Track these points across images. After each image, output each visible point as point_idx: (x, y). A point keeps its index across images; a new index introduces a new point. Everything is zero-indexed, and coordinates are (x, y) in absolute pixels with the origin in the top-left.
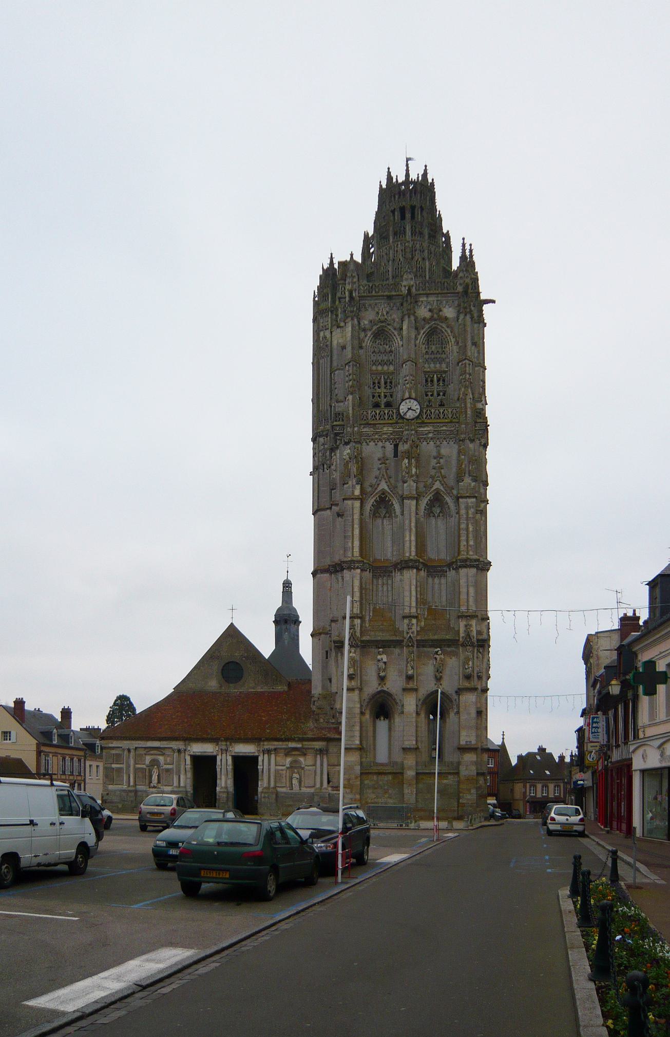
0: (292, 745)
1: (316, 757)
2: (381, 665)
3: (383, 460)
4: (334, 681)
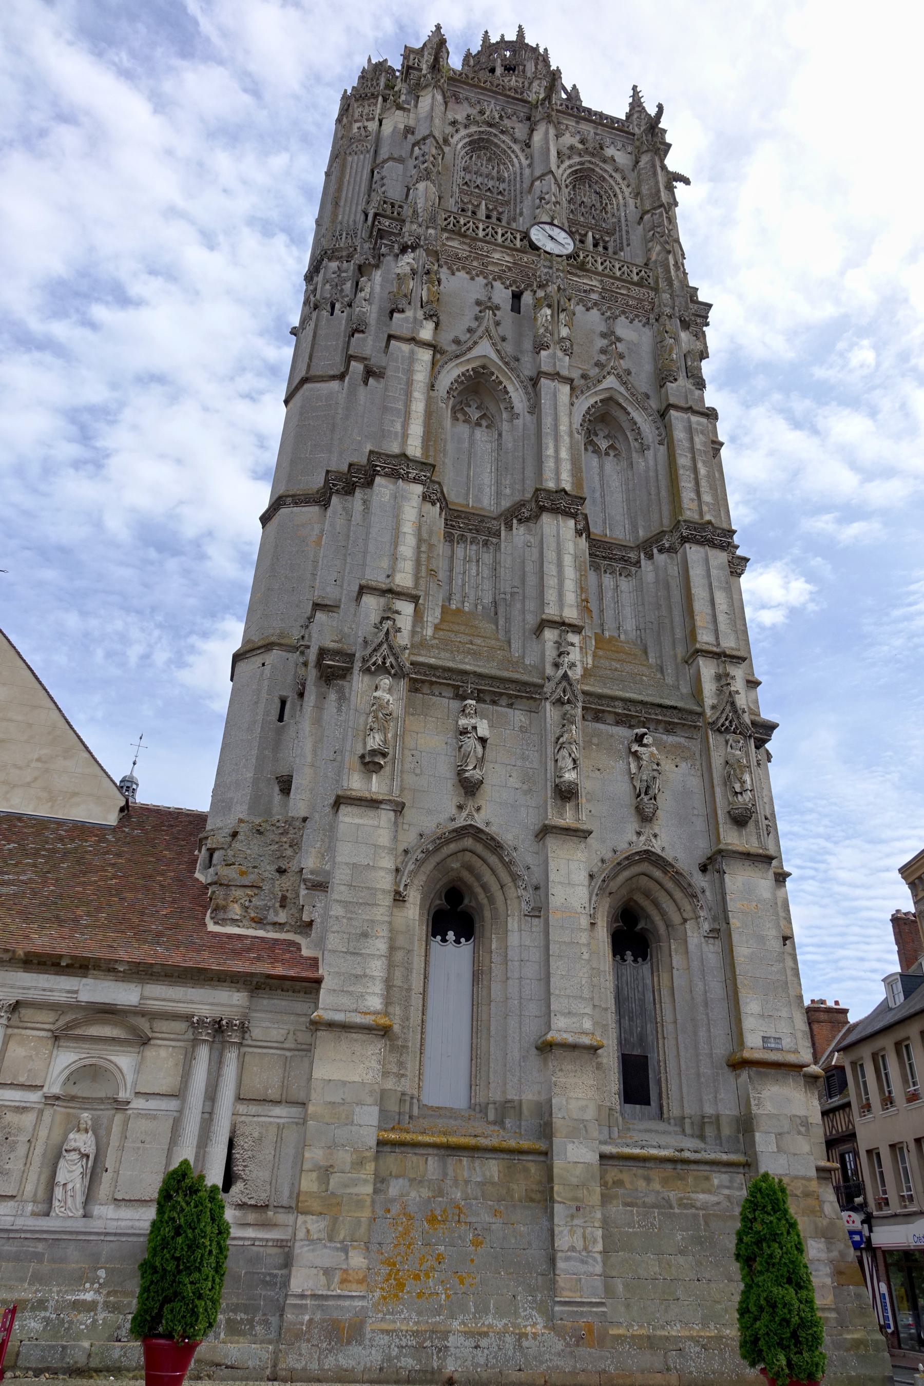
1: (189, 1059)
2: (471, 743)
3: (486, 305)
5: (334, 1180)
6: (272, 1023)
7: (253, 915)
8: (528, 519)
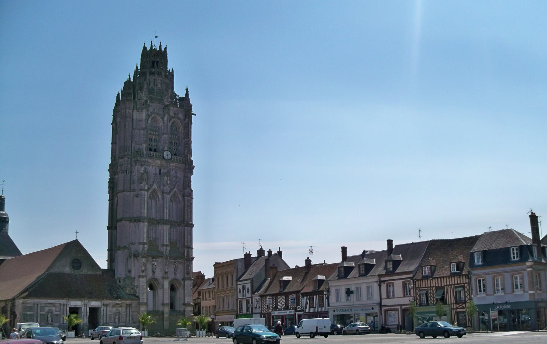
4: (133, 272)
6: (135, 303)
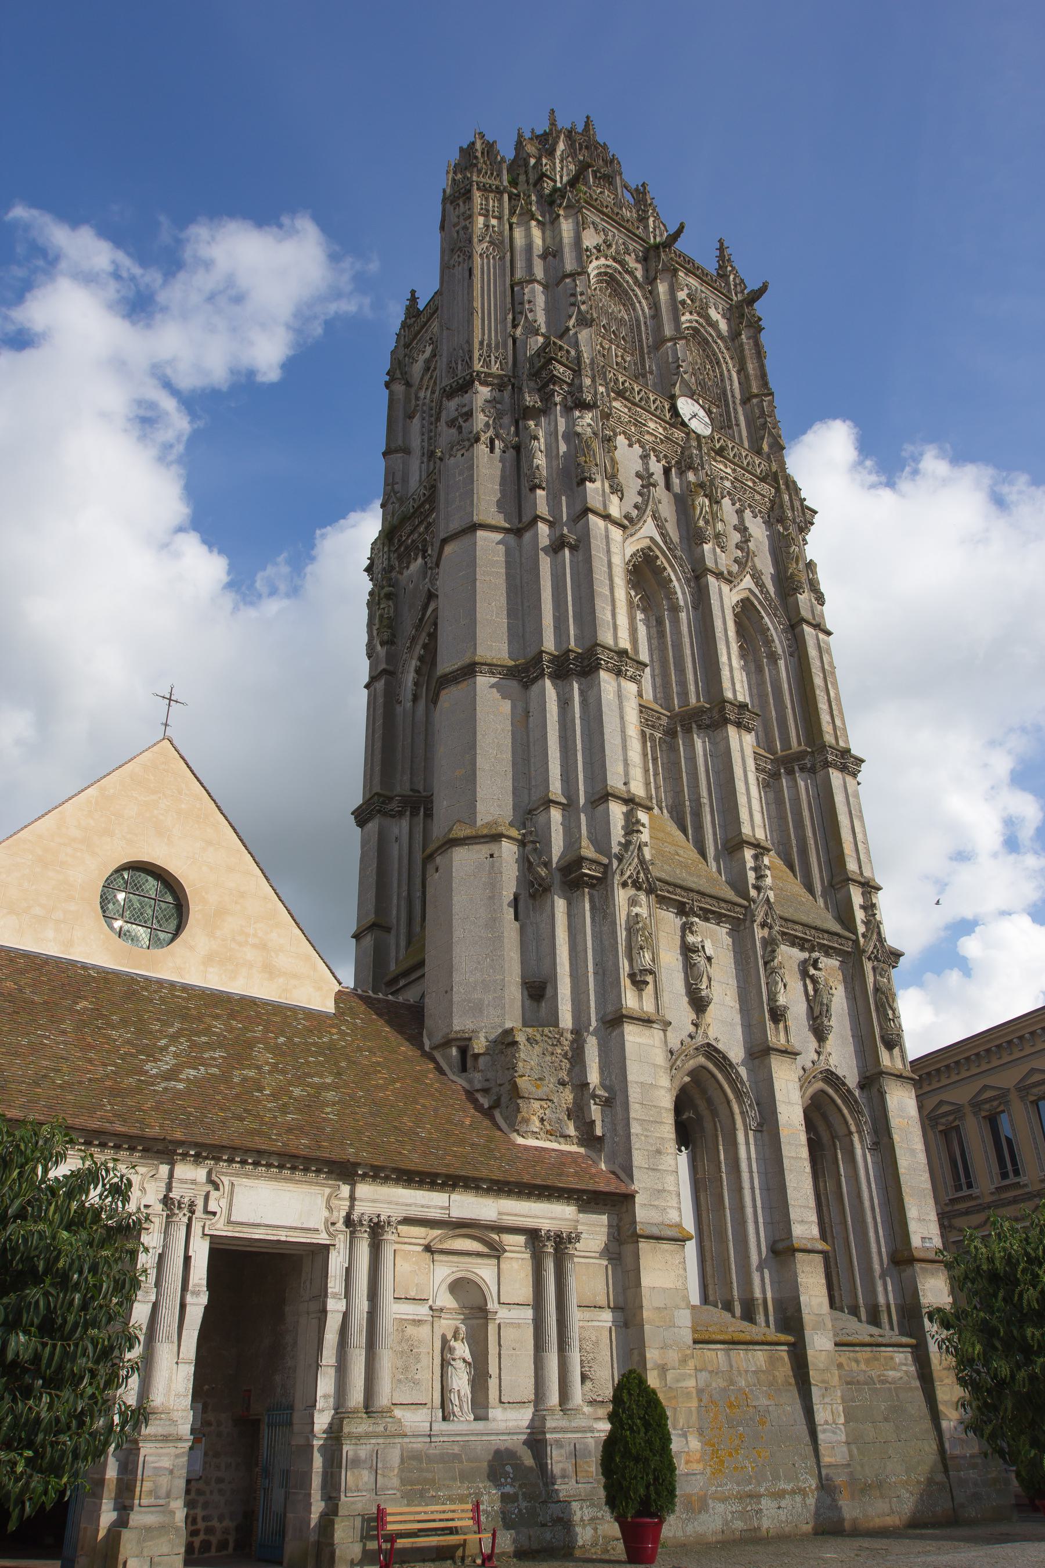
0: (467, 1205)
5: (670, 1375)
7: (548, 1127)
8: (708, 727)
